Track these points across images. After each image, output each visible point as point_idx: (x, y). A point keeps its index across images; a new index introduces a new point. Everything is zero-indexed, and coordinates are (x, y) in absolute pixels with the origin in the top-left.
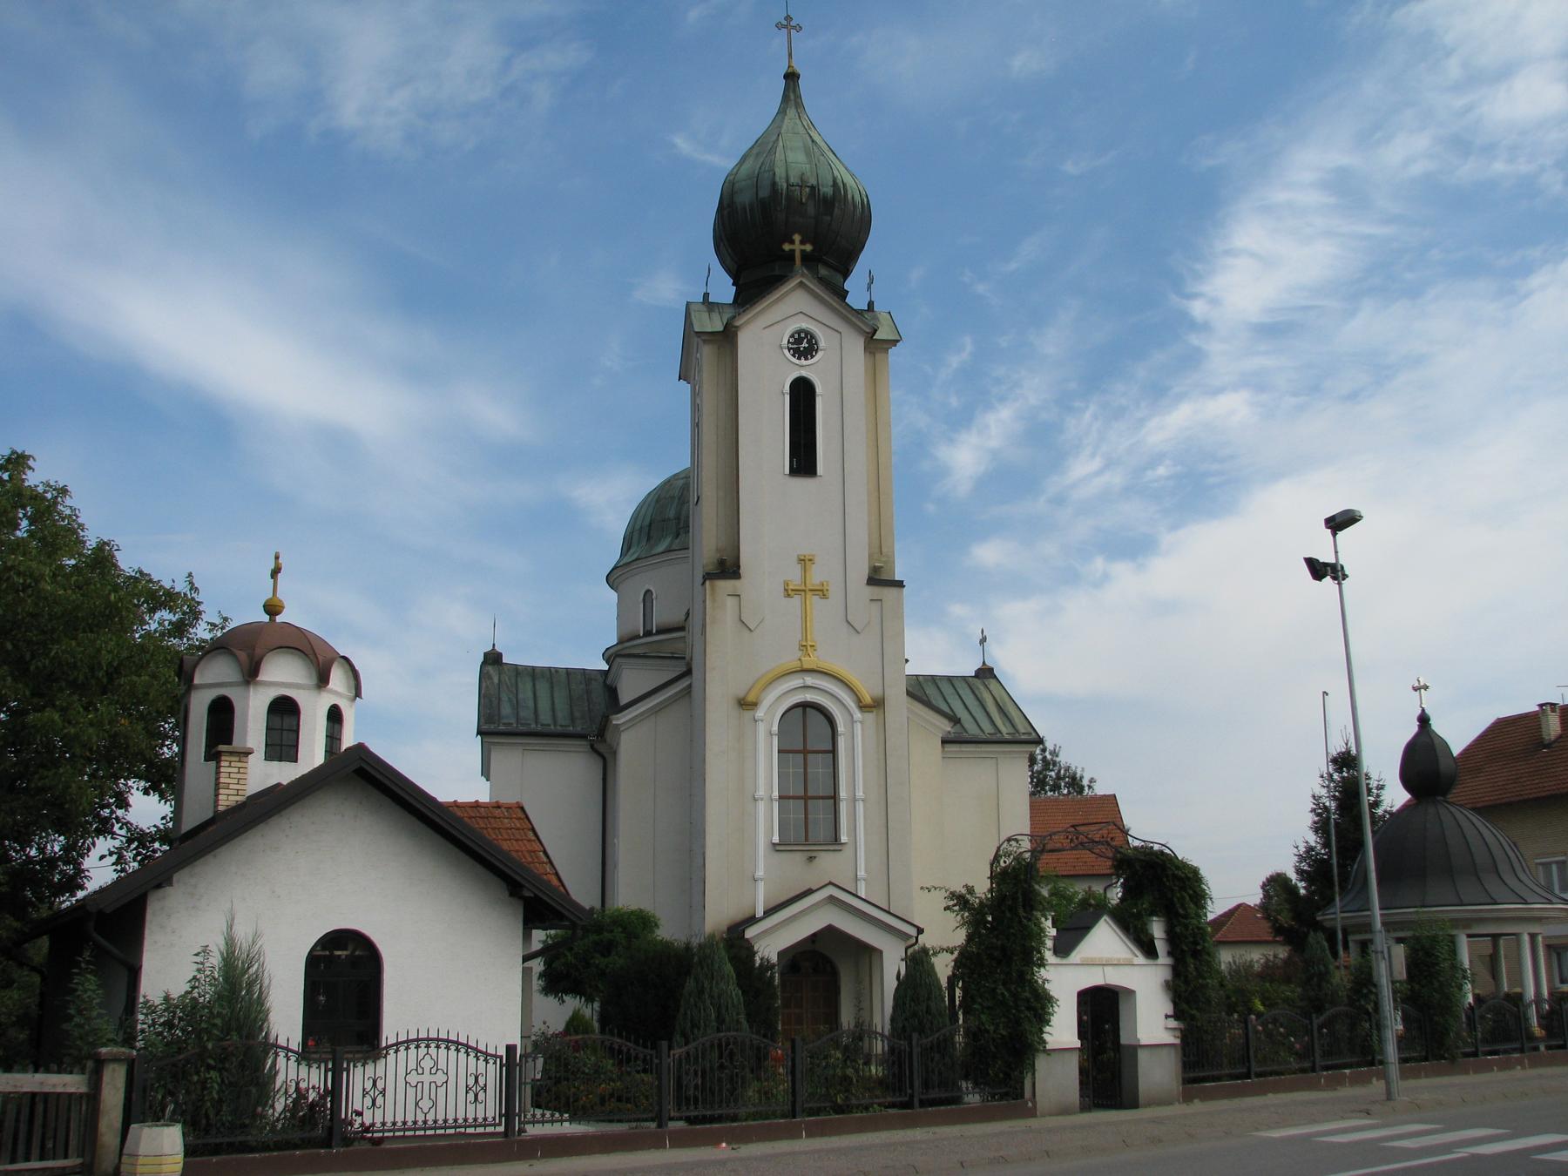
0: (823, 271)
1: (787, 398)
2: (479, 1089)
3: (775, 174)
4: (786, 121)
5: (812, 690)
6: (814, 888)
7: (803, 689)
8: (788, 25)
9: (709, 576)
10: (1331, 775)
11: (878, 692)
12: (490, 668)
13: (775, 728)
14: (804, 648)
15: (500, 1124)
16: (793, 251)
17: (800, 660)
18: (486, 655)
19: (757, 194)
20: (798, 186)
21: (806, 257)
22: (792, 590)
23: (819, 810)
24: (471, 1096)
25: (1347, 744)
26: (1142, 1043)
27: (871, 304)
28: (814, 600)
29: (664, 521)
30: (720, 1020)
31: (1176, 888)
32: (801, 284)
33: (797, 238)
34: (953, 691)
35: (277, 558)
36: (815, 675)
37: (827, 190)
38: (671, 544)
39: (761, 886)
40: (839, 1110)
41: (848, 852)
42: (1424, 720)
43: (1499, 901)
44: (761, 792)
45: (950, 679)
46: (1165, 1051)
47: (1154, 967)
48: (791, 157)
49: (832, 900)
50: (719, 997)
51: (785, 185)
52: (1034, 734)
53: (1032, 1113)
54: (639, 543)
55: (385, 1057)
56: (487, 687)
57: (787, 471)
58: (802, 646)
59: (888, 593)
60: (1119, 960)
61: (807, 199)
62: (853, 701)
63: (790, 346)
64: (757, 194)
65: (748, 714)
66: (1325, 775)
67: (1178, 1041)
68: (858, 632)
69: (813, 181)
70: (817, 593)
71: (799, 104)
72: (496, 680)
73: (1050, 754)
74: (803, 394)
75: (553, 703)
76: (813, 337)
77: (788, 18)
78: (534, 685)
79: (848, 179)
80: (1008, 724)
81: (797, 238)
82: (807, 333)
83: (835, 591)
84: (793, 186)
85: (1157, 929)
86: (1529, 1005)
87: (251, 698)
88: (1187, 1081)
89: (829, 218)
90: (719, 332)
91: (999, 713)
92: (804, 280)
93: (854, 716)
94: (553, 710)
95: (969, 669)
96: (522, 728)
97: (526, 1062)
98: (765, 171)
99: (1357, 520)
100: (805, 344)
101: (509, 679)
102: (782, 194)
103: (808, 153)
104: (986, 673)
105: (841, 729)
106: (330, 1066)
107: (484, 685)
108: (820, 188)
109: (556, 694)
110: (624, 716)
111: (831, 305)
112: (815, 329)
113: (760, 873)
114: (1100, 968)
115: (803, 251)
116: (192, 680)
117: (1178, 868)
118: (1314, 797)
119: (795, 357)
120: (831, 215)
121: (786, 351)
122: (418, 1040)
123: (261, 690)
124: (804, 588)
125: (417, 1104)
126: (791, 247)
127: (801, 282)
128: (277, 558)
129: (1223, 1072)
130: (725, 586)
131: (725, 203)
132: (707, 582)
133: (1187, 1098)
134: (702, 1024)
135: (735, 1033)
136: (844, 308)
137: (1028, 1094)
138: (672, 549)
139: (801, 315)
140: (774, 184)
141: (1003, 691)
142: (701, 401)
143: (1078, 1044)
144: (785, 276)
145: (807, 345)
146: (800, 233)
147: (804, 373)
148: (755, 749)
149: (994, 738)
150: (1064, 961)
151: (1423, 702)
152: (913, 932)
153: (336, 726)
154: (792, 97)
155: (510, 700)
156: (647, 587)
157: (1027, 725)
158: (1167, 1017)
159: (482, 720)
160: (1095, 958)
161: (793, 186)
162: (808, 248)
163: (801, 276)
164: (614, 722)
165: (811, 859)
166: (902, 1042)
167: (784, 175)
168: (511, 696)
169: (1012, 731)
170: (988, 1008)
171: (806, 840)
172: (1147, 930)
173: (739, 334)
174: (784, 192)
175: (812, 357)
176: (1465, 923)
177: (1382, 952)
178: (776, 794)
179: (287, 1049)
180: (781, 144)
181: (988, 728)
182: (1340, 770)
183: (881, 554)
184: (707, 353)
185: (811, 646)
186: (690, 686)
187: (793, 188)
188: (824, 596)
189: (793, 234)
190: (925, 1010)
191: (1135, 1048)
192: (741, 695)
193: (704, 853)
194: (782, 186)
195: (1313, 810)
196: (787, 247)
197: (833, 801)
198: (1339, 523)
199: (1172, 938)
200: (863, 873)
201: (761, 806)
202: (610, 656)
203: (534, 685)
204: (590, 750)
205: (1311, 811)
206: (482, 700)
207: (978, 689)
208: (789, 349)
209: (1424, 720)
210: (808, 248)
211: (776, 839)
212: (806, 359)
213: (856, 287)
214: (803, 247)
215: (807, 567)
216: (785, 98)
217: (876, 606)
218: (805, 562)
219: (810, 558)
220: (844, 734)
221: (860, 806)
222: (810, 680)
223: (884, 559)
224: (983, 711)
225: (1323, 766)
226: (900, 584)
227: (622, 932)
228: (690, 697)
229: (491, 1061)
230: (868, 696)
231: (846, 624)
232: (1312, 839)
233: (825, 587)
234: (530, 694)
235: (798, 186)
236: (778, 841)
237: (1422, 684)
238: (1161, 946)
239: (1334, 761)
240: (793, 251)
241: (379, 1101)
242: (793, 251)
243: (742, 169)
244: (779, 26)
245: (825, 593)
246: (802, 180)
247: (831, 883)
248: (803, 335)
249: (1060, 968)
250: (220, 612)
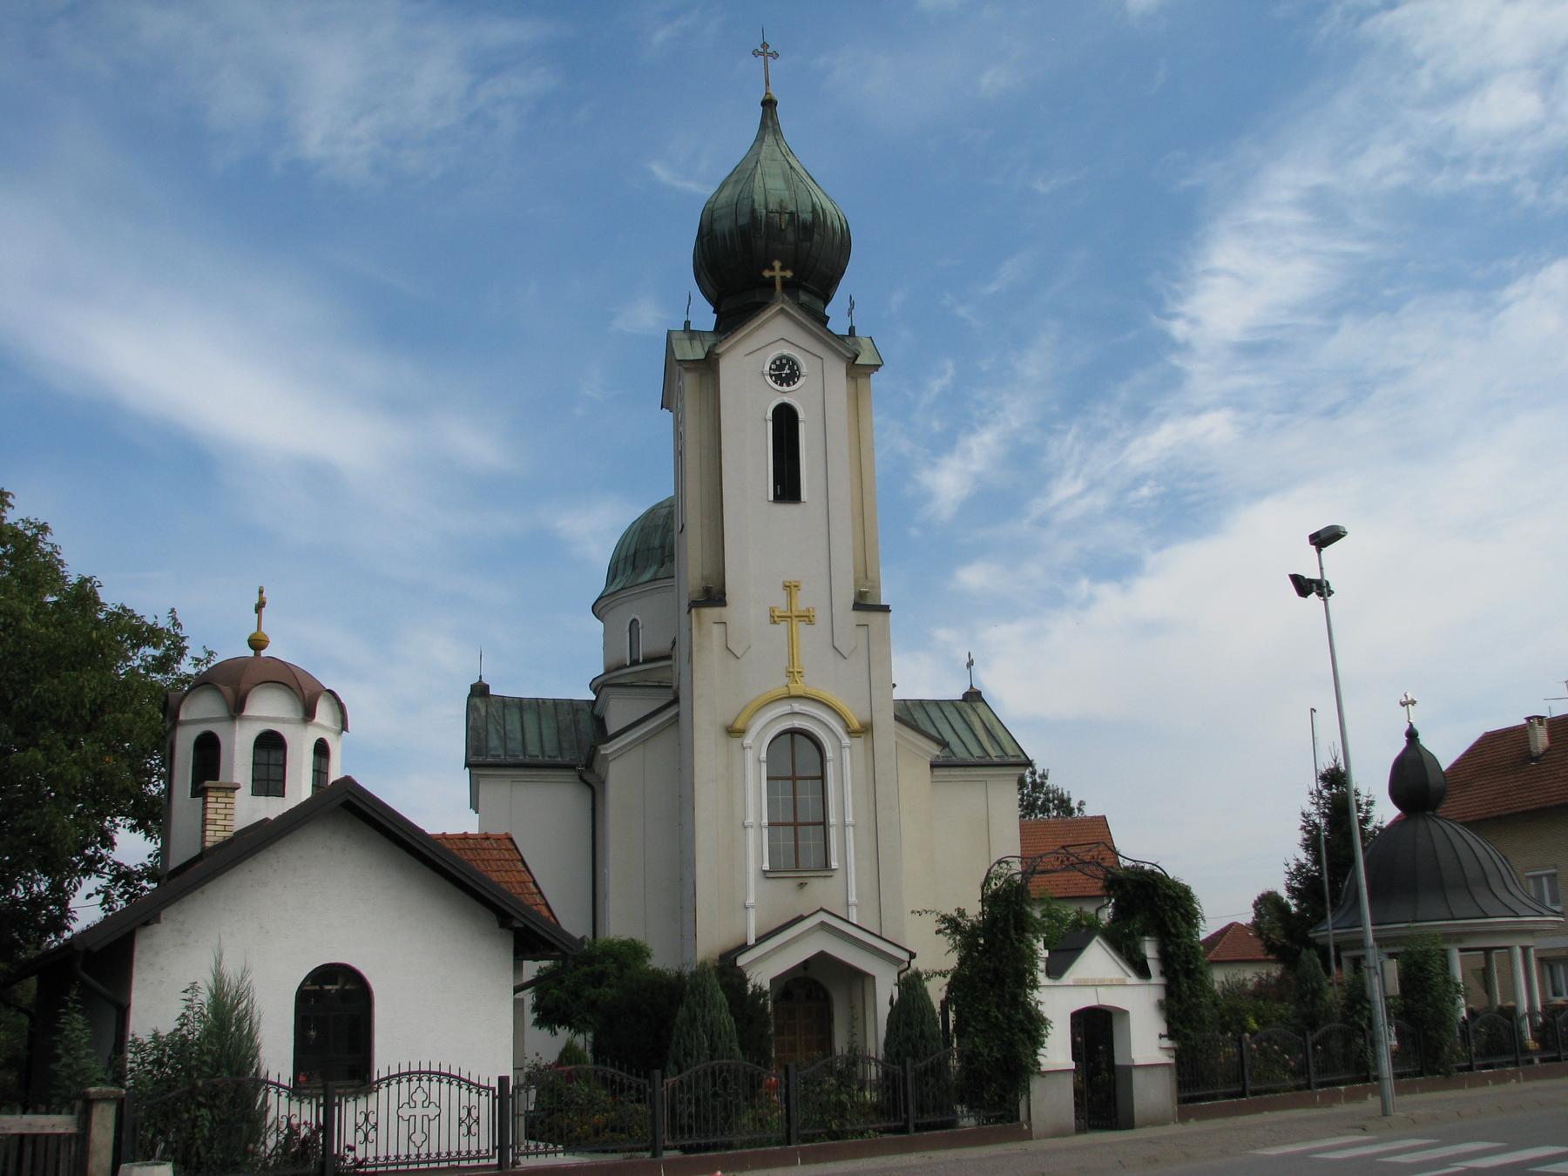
0: (804, 297)
1: (770, 424)
2: (467, 1121)
3: (753, 201)
4: (764, 147)
5: (798, 717)
6: (805, 915)
7: (790, 716)
8: (765, 52)
9: (695, 604)
10: (1320, 792)
11: (866, 717)
12: (477, 701)
13: (764, 755)
15: (493, 1157)
16: (774, 277)
17: (787, 686)
18: (473, 687)
19: (736, 223)
20: (778, 212)
21: (786, 284)
22: (778, 617)
23: (810, 837)
24: (464, 1129)
25: (1335, 761)
26: (1138, 1062)
27: (852, 330)
28: (800, 627)
29: (649, 550)
30: (713, 1048)
31: (1168, 908)
32: (782, 311)
33: (777, 264)
34: (942, 716)
35: (261, 592)
36: (803, 701)
37: (807, 216)
38: (656, 573)
39: (752, 915)
40: (834, 1136)
41: (838, 877)
42: (1412, 735)
43: (1490, 915)
44: (750, 820)
45: (937, 703)
46: (1159, 1071)
47: (1147, 988)
48: (770, 184)
49: (823, 925)
50: (711, 1024)
51: (764, 212)
52: (1023, 757)
53: (1028, 1135)
54: (624, 574)
55: (377, 1091)
56: (474, 719)
57: (771, 498)
58: (789, 672)
59: (875, 618)
60: (1111, 980)
61: (787, 225)
62: (841, 727)
63: (772, 372)
64: (736, 223)
65: (736, 742)
66: (1315, 792)
67: (1172, 1061)
68: (845, 658)
69: (792, 208)
70: (802, 619)
71: (777, 131)
72: (483, 712)
73: (1040, 777)
74: (785, 421)
75: (541, 735)
76: (794, 363)
77: (765, 46)
78: (522, 717)
79: (828, 206)
80: (996, 746)
81: (777, 264)
82: (789, 359)
83: (821, 616)
84: (772, 212)
85: (1150, 949)
86: (1523, 1018)
87: (237, 733)
88: (1182, 1101)
89: (808, 244)
90: (700, 360)
91: (988, 737)
92: (785, 307)
94: (541, 741)
95: (956, 693)
96: (510, 760)
97: (519, 1093)
98: (744, 198)
99: (1344, 536)
100: (787, 371)
101: (497, 712)
102: (761, 220)
103: (787, 180)
104: (973, 696)
105: (829, 754)
106: (321, 1101)
107: (471, 717)
108: (800, 214)
109: (544, 725)
110: (611, 746)
111: (812, 330)
112: (797, 356)
113: (751, 901)
114: (1093, 989)
115: (782, 278)
116: (177, 716)
117: (1169, 887)
118: (1303, 814)
119: (777, 383)
120: (811, 239)
121: (768, 378)
122: (409, 1073)
123: (246, 725)
124: (789, 614)
125: (409, 1138)
126: (772, 274)
127: (782, 309)
128: (261, 592)
129: (1218, 1091)
130: (710, 613)
131: (705, 230)
132: (693, 610)
133: (1183, 1117)
134: (695, 1052)
135: (728, 1061)
136: (826, 334)
138: (658, 577)
139: (782, 341)
140: (753, 211)
141: (991, 714)
142: (684, 430)
143: (1072, 1065)
144: (766, 303)
145: (788, 372)
146: (780, 260)
147: (786, 399)
148: (744, 775)
149: (982, 761)
150: (1057, 983)
151: (1411, 717)
152: (905, 956)
153: (323, 760)
154: (770, 124)
155: (498, 732)
156: (633, 616)
157: (1017, 749)
158: (1161, 1036)
159: (470, 753)
161: (772, 212)
162: (789, 274)
163: (781, 302)
164: (602, 752)
165: (802, 885)
166: (896, 1067)
167: (763, 203)
168: (498, 728)
169: (1000, 753)
170: (982, 1031)
171: (797, 867)
172: (1139, 950)
173: (720, 360)
174: (763, 223)
175: (794, 383)
176: (1456, 937)
177: (1375, 968)
178: (765, 821)
179: (278, 1085)
180: (759, 171)
181: (977, 751)
182: (1329, 787)
183: (867, 578)
184: (689, 381)
186: (678, 714)
187: (772, 215)
188: (811, 622)
189: (774, 261)
190: (918, 1034)
191: (1129, 1069)
192: (729, 722)
193: (695, 882)
194: (760, 213)
195: (1303, 828)
196: (767, 274)
197: (822, 827)
198: (1323, 539)
199: (1165, 958)
200: (854, 899)
201: (751, 833)
202: (598, 686)
203: (522, 717)
204: (579, 781)
205: (1301, 829)
206: (470, 732)
207: (965, 712)
208: (771, 376)
209: (1412, 735)
210: (789, 274)
211: (766, 866)
212: (788, 385)
213: (837, 314)
214: (783, 274)
215: (793, 594)
216: (763, 125)
217: (862, 632)
218: (791, 588)
219: (796, 584)
220: (832, 760)
221: (850, 832)
222: (797, 706)
223: (869, 584)
224: (972, 735)
225: (1312, 783)
226: (886, 609)
227: (614, 963)
228: (678, 725)
229: (484, 1094)
230: (855, 721)
231: (833, 650)
232: (1303, 856)
233: (811, 614)
234: (518, 727)
235: (778, 212)
236: (768, 869)
237: (1409, 699)
238: (1153, 966)
239: (1323, 778)
240: (773, 278)
241: (372, 1135)
242: (773, 278)
243: (722, 195)
244: (756, 53)
245: (811, 618)
246: (781, 207)
247: (822, 909)
248: (784, 361)
250: (204, 647)
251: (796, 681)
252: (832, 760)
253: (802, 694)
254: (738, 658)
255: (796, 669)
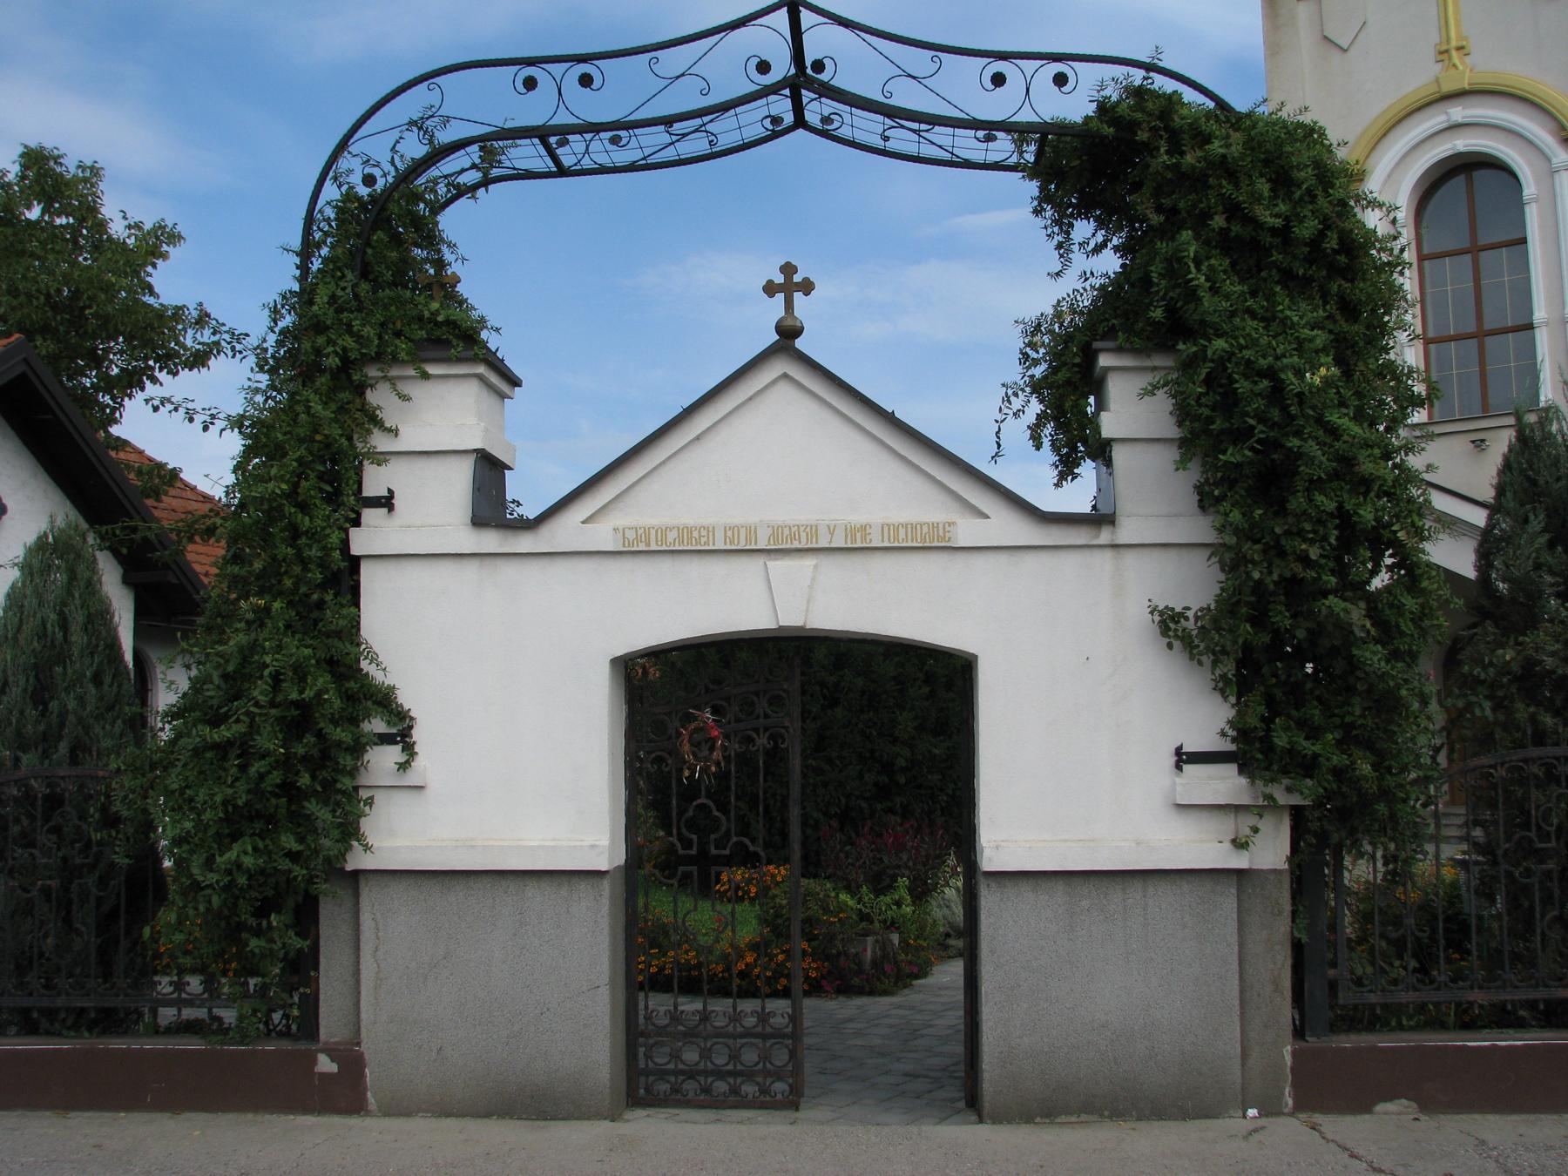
7: (1447, 135)
14: (1445, 57)
46: (1164, 902)
47: (1104, 560)
58: (1441, 53)
62: (1550, 132)
93: (1554, 160)
114: (756, 563)
137: (330, 1025)
160: (711, 530)
171: (1485, 406)
185: (1459, 49)
222: (1458, 113)
249: (510, 570)
251: (1455, 66)
252: (1536, 200)
253: (1467, 87)
254: (1345, 51)
255: (1454, 43)
